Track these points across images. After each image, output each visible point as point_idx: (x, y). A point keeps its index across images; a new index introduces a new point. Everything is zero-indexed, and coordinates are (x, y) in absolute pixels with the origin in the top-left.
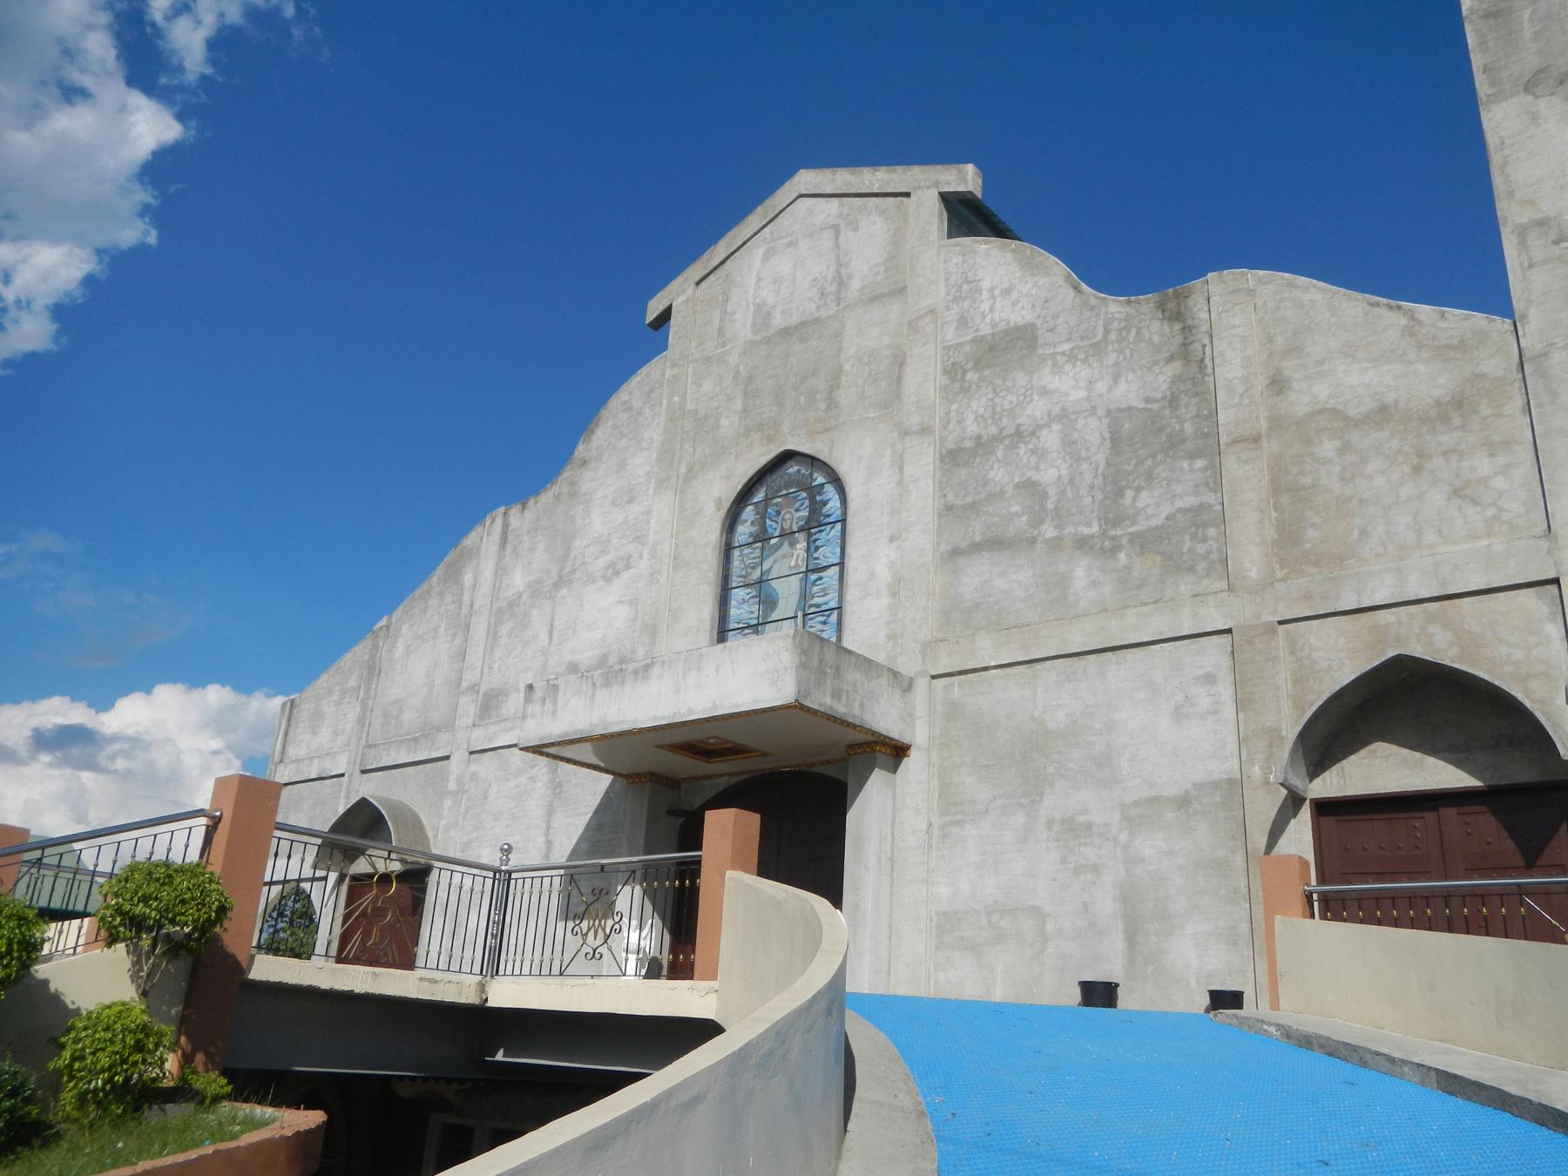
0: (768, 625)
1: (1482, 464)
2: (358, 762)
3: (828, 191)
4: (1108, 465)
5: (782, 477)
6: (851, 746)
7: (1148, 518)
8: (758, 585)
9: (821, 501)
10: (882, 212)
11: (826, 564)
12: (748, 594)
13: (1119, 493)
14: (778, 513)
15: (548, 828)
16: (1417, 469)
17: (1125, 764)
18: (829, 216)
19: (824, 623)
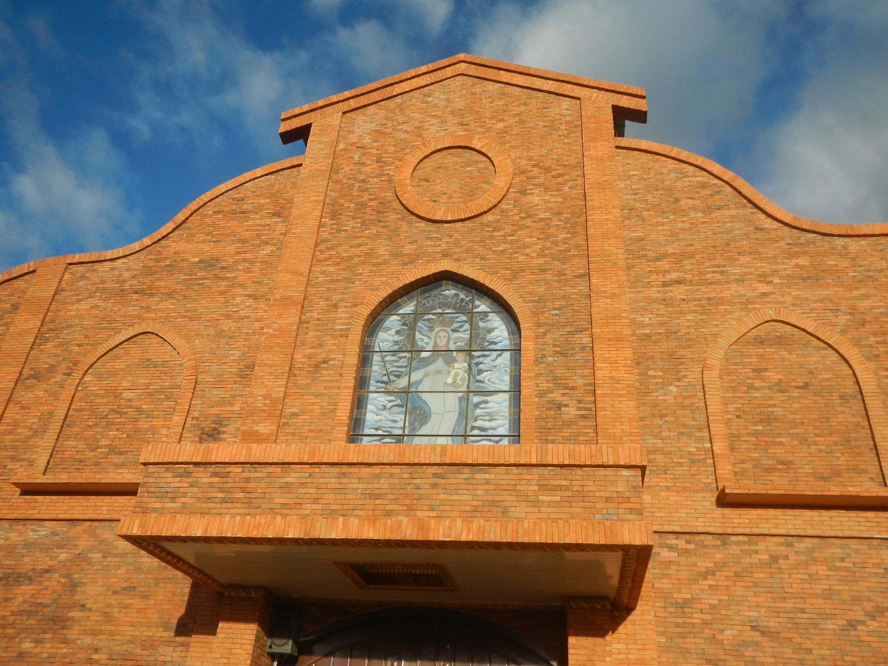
0: (416, 437)
5: (435, 296)
6: (573, 598)
9: (484, 328)
11: (491, 389)
12: (390, 401)
14: (431, 329)
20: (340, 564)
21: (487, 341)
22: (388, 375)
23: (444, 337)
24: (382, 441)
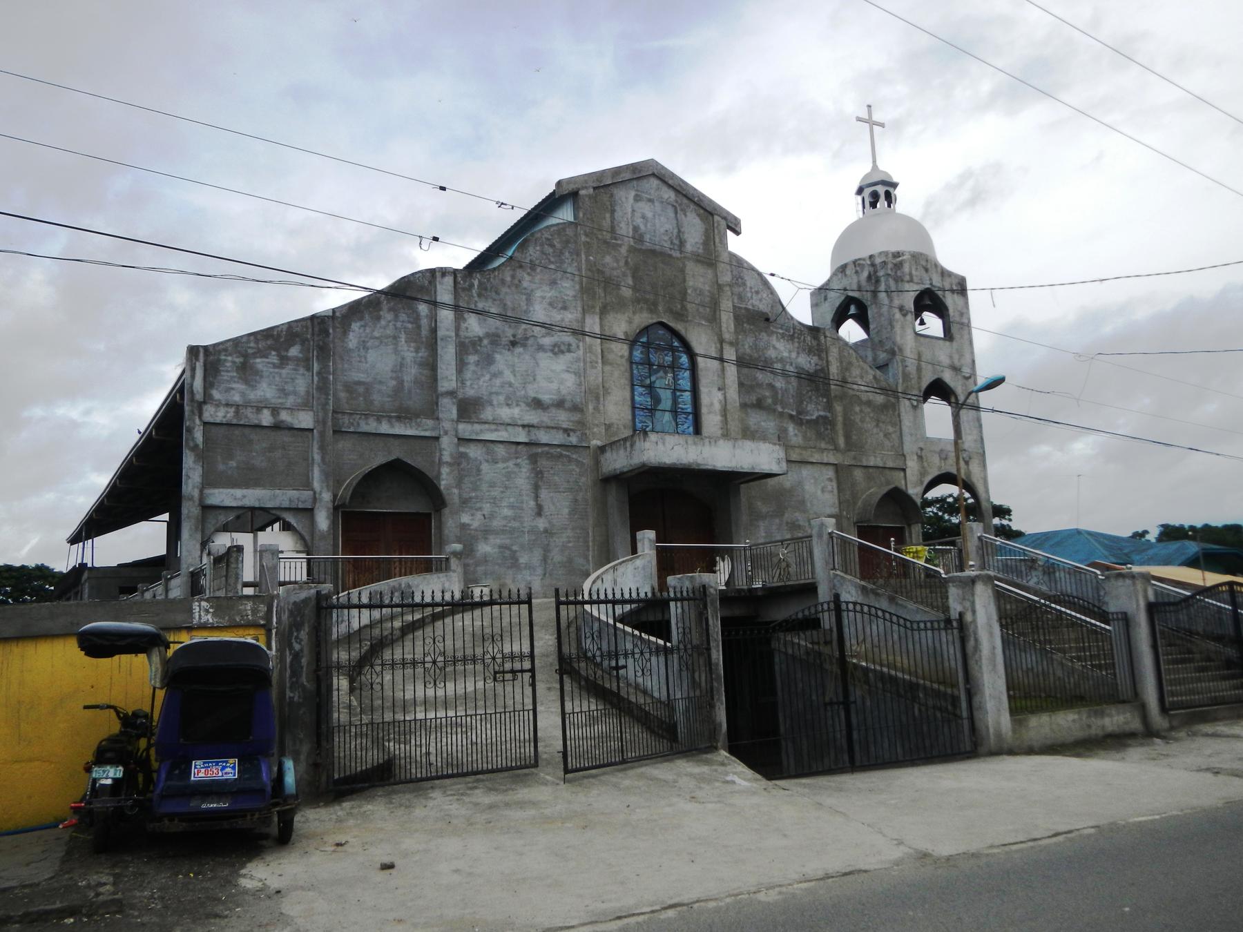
1: (891, 429)
2: (330, 423)
3: (670, 182)
4: (798, 389)
7: (812, 415)
10: (699, 215)
13: (801, 402)
15: (537, 497)
16: (877, 426)
17: (809, 505)
18: (670, 197)
19: (686, 418)
22: (640, 376)
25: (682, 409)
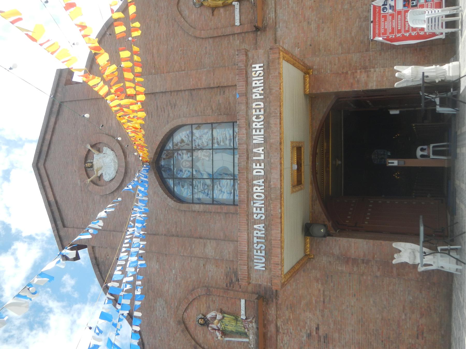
6: (305, 91)
8: (215, 181)
11: (211, 138)
12: (217, 187)
14: (181, 171)
20: (293, 192)
21: (188, 141)
23: (185, 163)
24: (237, 189)
25: (230, 140)
